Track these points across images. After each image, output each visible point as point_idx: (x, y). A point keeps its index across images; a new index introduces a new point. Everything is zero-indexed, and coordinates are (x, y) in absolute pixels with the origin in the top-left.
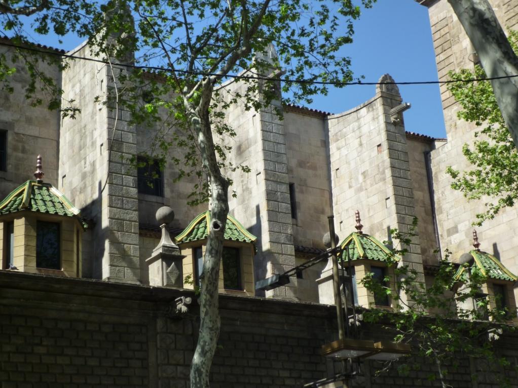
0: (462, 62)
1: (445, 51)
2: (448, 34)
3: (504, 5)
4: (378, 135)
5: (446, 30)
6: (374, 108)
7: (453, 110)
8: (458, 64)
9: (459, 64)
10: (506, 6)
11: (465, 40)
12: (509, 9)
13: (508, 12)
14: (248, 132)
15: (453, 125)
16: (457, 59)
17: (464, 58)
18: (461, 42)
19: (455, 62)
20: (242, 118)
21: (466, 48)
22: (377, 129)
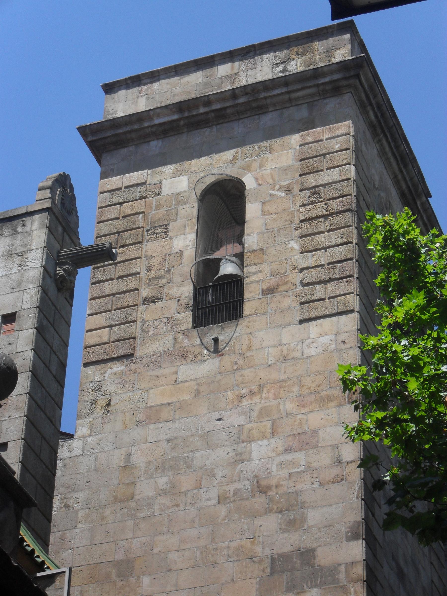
0: (163, 277)
1: (123, 246)
2: (141, 216)
3: (301, 190)
5: (139, 206)
6: (19, 229)
7: (109, 371)
8: (150, 280)
9: (151, 281)
10: (307, 193)
11: (182, 237)
12: (313, 199)
13: (311, 206)
15: (102, 401)
16: (149, 270)
17: (169, 271)
18: (171, 238)
19: (144, 273)
21: (180, 254)
22: (15, 277)
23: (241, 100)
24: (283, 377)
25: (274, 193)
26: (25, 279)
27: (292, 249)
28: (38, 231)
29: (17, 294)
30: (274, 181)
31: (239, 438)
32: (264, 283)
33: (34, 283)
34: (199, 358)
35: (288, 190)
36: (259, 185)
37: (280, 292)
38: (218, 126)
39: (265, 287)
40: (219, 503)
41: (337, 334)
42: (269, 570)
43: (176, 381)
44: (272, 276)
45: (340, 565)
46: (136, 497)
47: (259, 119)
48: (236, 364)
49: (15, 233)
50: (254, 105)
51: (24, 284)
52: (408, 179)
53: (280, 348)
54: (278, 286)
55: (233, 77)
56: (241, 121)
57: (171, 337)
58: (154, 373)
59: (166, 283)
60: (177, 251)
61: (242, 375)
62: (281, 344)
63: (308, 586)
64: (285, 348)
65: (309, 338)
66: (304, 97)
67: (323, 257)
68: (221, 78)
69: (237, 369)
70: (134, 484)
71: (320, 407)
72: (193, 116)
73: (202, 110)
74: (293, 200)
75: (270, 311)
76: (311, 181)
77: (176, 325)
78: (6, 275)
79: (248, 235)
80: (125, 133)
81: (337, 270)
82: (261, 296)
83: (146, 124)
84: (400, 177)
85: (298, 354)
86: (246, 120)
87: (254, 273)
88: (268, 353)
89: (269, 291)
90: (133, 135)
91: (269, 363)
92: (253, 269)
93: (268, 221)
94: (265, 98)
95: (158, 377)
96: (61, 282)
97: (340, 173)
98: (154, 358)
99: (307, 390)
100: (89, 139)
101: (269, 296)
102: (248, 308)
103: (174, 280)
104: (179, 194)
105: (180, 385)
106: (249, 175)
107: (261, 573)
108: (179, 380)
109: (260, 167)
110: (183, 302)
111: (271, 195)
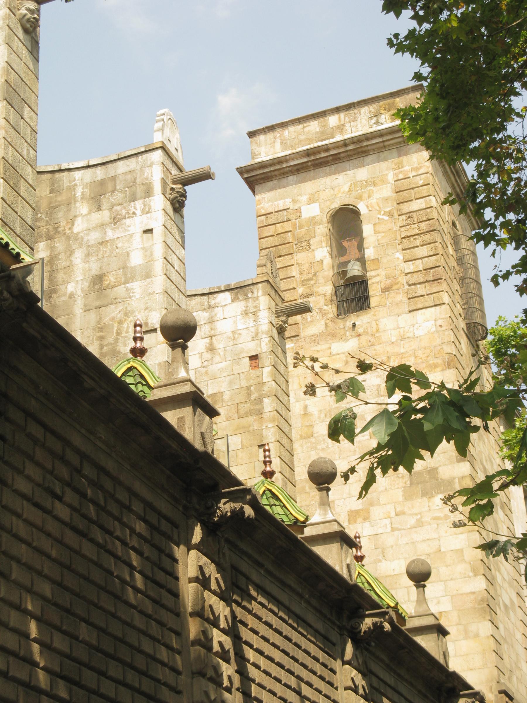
0: (312, 279)
1: (280, 256)
2: (289, 233)
3: (400, 215)
4: (253, 339)
5: (288, 226)
6: (250, 295)
8: (302, 281)
9: (304, 282)
10: (404, 217)
12: (409, 222)
13: (408, 227)
14: (128, 256)
16: (301, 274)
17: (315, 275)
19: (297, 276)
20: (114, 229)
21: (321, 262)
22: (253, 330)
23: (351, 147)
24: (402, 351)
25: (381, 217)
26: (260, 331)
27: (398, 259)
28: (263, 297)
29: (256, 341)
30: (380, 208)
31: (378, 393)
32: (382, 284)
33: (267, 334)
34: (344, 337)
35: (390, 215)
36: (370, 211)
37: (394, 290)
38: (335, 165)
39: (383, 287)
40: (371, 438)
41: (436, 320)
42: (409, 482)
43: (331, 354)
44: (386, 278)
45: (454, 478)
46: (315, 435)
47: (363, 160)
48: (370, 342)
49: (246, 298)
50: (359, 150)
51: (260, 335)
52: (460, 185)
53: (398, 330)
54: (392, 286)
55: (341, 128)
56: (351, 161)
57: (323, 322)
58: (316, 348)
59: (315, 283)
60: (318, 260)
61: (375, 350)
62: (399, 328)
63: (435, 493)
64: (401, 330)
65: (417, 323)
66: (394, 144)
67: (420, 265)
68: (332, 128)
69: (371, 345)
70: (312, 426)
71: (429, 371)
72: (317, 159)
73: (323, 155)
74: (395, 223)
75: (388, 304)
76: (406, 208)
77: (326, 314)
78: (246, 328)
79: (367, 248)
80: (270, 172)
81: (431, 275)
82: (381, 293)
83: (284, 165)
84: (456, 185)
85: (411, 335)
86: (354, 161)
87: (375, 276)
88: (391, 334)
89: (386, 290)
90: (276, 173)
91: (393, 341)
92: (373, 273)
93: (379, 238)
94: (367, 146)
95: (318, 351)
96: (280, 329)
97: (426, 202)
98: (314, 338)
99: (420, 360)
100: (246, 176)
101: (386, 293)
102: (373, 302)
103: (320, 282)
104: (314, 217)
105: (334, 357)
106: (362, 203)
107: (404, 485)
108: (333, 353)
109: (369, 197)
110: (329, 297)
111: (379, 218)
